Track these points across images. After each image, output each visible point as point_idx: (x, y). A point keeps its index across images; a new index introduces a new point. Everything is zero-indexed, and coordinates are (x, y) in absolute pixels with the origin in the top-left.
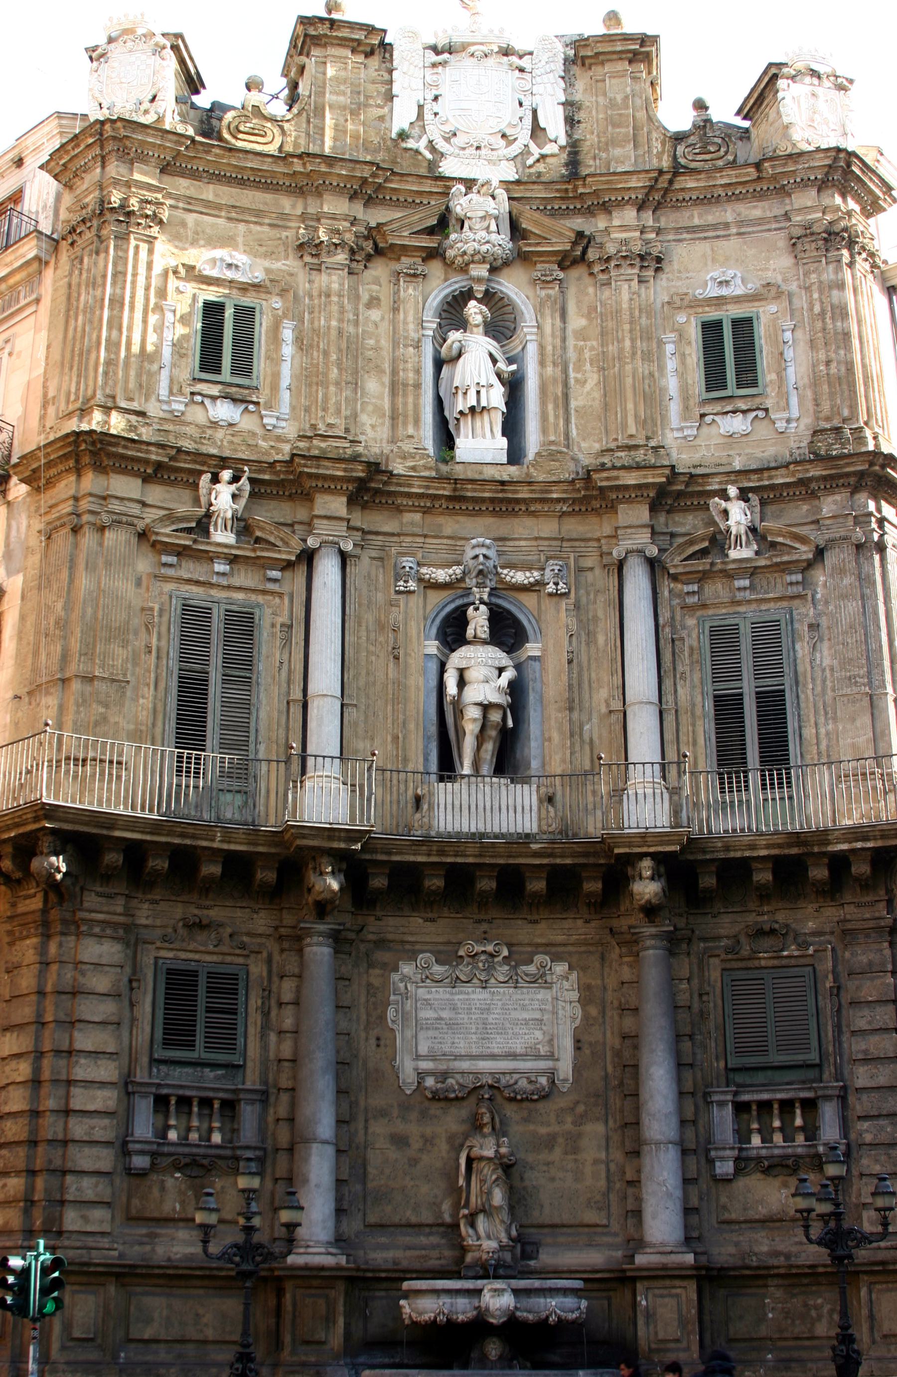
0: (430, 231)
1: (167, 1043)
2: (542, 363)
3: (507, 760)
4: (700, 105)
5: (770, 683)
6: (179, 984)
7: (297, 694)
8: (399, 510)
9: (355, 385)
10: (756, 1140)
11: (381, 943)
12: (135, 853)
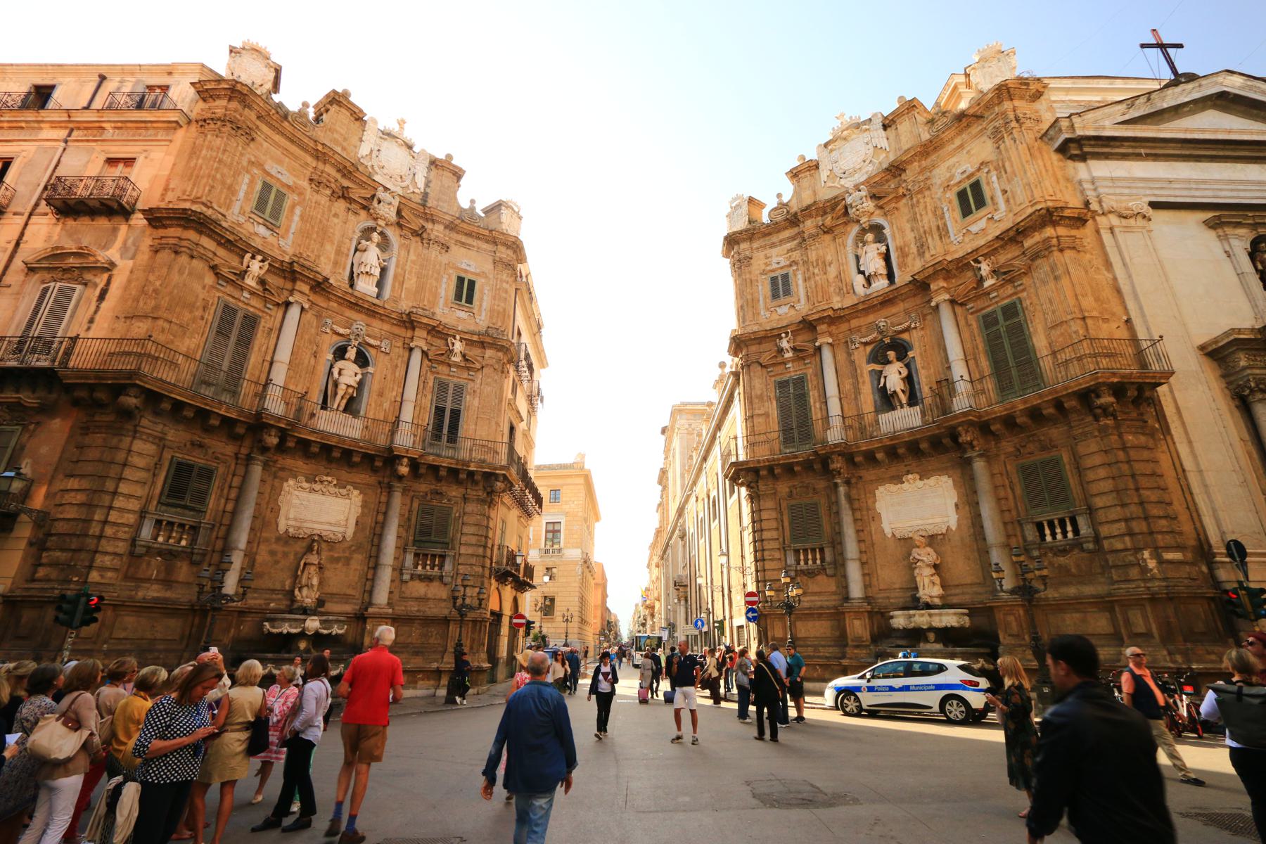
0: (365, 199)
1: (169, 496)
2: (397, 266)
3: (351, 407)
4: (473, 201)
5: (456, 407)
7: (268, 358)
8: (329, 299)
9: (322, 245)
10: (420, 568)
11: (282, 469)
12: (178, 406)
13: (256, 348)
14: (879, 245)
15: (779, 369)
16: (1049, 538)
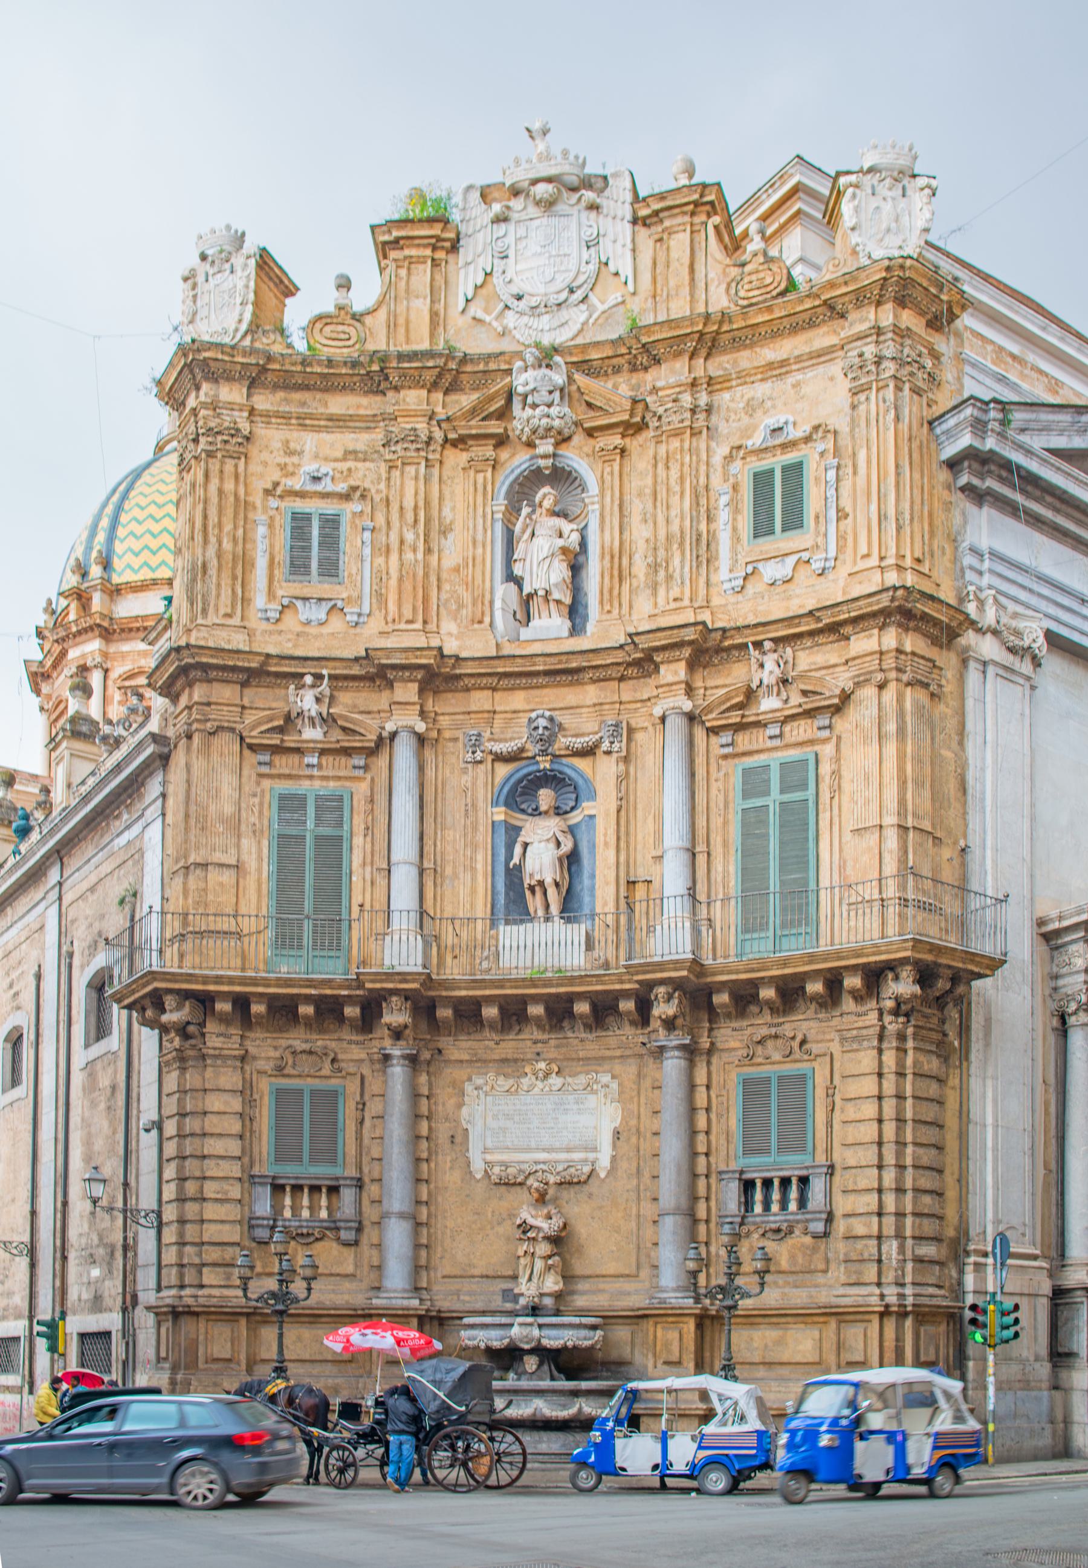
14: (566, 527)
15: (284, 764)
16: (758, 1208)
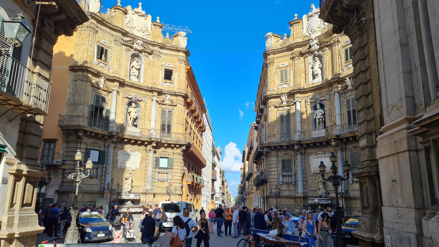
6: (283, 162)
11: (308, 153)
12: (275, 147)
13: (292, 121)
